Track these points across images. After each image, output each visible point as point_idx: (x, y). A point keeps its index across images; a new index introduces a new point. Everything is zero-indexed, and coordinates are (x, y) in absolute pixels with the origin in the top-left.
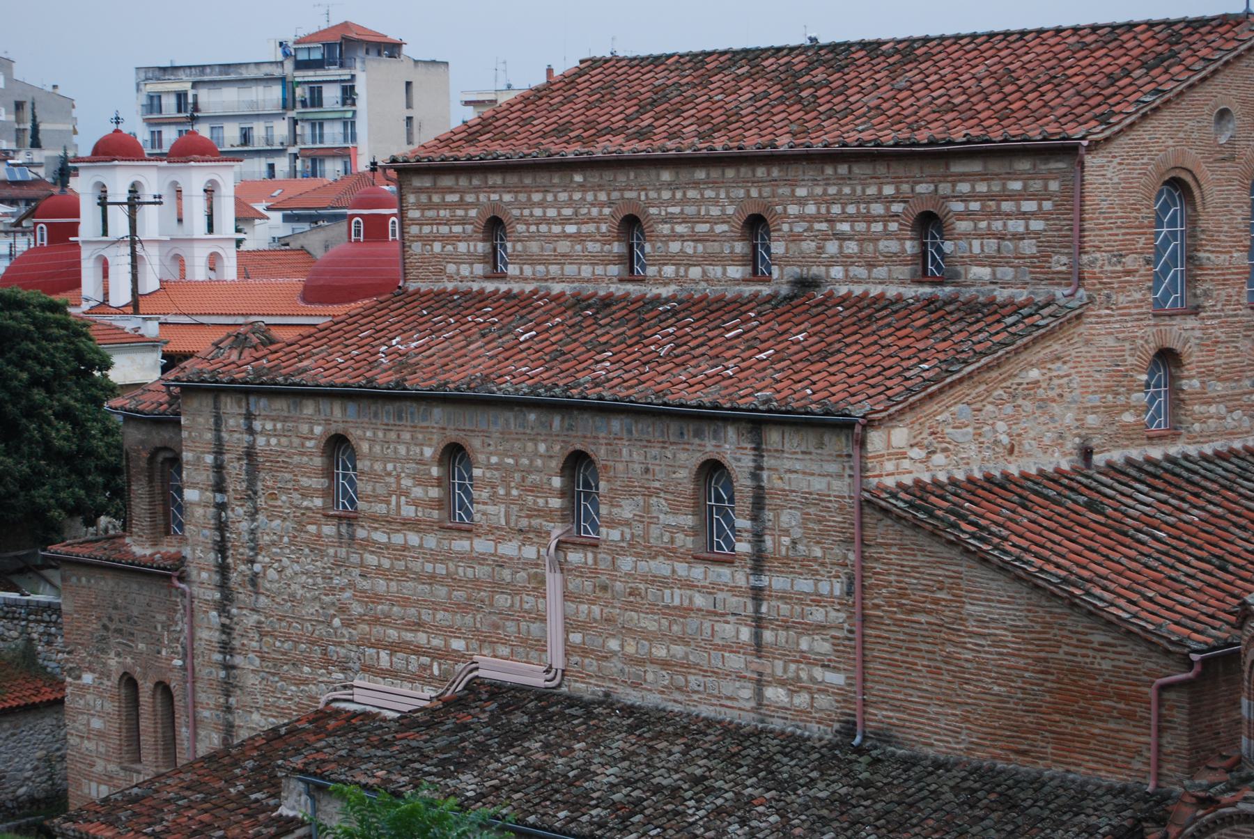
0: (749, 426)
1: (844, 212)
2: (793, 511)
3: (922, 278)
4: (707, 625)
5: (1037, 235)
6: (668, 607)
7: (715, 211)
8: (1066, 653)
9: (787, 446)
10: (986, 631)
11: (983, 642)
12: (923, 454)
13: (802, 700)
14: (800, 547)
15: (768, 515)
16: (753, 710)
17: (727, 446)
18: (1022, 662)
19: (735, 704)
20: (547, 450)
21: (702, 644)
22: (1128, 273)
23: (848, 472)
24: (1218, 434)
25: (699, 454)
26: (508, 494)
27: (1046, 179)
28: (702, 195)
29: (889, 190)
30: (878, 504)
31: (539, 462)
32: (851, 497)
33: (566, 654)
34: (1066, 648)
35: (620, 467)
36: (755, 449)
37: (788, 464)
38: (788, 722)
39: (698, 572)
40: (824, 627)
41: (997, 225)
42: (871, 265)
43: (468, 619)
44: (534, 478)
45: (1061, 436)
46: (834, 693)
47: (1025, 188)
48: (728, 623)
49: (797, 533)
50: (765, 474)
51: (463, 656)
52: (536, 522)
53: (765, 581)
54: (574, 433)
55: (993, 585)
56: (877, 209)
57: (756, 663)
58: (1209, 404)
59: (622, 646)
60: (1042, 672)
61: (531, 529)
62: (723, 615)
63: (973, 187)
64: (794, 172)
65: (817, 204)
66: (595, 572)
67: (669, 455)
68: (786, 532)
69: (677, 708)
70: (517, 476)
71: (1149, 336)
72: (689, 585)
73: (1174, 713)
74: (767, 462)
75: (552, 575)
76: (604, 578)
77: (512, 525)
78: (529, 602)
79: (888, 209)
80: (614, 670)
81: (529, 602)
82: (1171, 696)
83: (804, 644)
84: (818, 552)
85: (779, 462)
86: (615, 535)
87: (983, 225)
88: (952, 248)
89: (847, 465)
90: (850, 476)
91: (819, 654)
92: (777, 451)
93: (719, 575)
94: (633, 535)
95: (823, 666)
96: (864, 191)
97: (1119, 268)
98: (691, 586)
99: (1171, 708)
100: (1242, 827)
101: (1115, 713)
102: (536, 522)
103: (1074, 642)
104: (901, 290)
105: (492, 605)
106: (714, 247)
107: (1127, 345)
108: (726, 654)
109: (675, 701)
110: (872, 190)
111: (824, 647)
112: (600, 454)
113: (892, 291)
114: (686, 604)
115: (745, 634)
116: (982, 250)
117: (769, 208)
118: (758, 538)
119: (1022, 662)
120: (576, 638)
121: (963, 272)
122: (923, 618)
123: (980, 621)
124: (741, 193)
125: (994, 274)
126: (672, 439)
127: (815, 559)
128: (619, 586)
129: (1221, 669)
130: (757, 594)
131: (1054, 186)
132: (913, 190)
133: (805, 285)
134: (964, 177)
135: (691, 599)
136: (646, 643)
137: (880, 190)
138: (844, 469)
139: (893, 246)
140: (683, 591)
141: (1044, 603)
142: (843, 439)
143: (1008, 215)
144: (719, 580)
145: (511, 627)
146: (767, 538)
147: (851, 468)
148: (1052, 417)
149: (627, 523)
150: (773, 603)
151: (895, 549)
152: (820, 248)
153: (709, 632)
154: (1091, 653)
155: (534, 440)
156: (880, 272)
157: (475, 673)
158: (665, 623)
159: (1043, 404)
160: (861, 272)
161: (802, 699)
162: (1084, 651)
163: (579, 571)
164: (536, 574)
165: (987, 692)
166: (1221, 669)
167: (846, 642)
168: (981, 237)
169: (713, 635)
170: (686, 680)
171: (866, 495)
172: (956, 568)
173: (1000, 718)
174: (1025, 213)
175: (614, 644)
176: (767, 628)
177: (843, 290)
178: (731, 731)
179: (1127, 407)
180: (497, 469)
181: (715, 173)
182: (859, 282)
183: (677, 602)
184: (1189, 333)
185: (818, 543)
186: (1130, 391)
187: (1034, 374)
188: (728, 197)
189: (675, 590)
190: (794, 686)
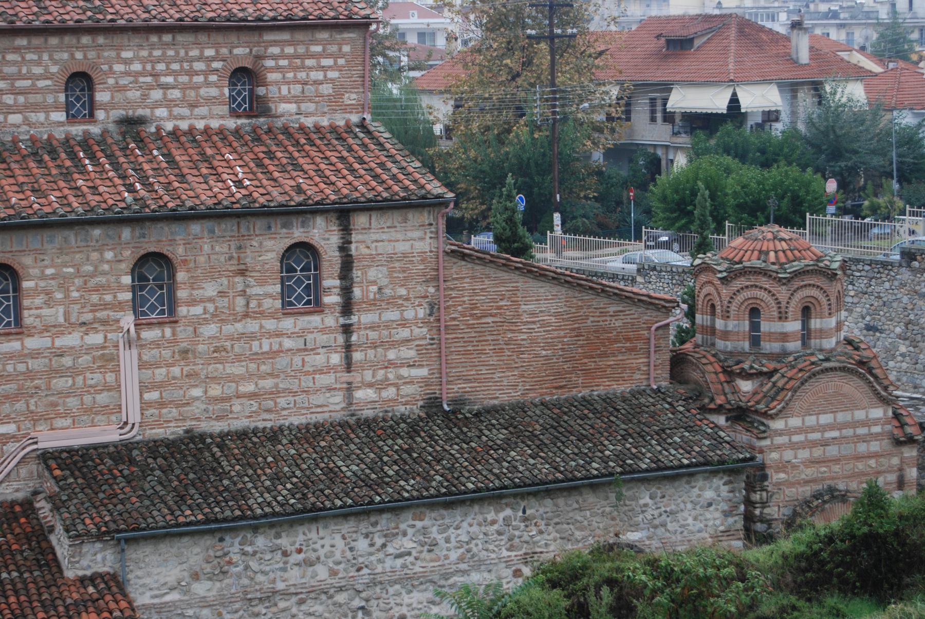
0: (336, 215)
1: (168, 68)
2: (380, 268)
3: (234, 114)
4: (297, 360)
5: (332, 80)
6: (256, 354)
7: (38, 70)
8: (592, 322)
9: (373, 226)
10: (537, 319)
11: (534, 326)
13: (390, 392)
14: (388, 291)
15: (357, 273)
16: (343, 409)
17: (316, 231)
18: (562, 333)
19: (325, 409)
20: (116, 257)
21: (293, 373)
23: (429, 235)
25: (287, 240)
26: (67, 296)
27: (340, 44)
28: (23, 58)
29: (209, 52)
30: (462, 253)
31: (106, 267)
32: (431, 252)
33: (142, 409)
34: (592, 319)
35: (202, 259)
36: (342, 230)
37: (374, 237)
38: (376, 411)
39: (288, 324)
40: (408, 341)
41: (302, 75)
42: (192, 106)
43: (20, 405)
44: (102, 280)
46: (418, 382)
47: (324, 50)
48: (319, 354)
49: (384, 282)
50: (353, 246)
51: (14, 437)
52: (101, 315)
53: (354, 319)
54: (146, 240)
55: (542, 290)
56: (199, 66)
57: (346, 377)
59: (206, 392)
60: (577, 336)
61: (95, 320)
62: (312, 350)
63: (282, 50)
64: (118, 40)
65: (143, 61)
66: (174, 341)
67: (255, 243)
68: (374, 283)
69: (269, 425)
70: (78, 282)
72: (279, 334)
73: (661, 341)
74: (355, 237)
75: (128, 352)
76: (184, 344)
77: (73, 320)
78: (95, 378)
79: (208, 66)
80: (196, 411)
81: (95, 378)
82: (660, 332)
83: (391, 355)
84: (403, 291)
85: (366, 236)
86: (198, 310)
87: (290, 75)
88: (265, 92)
89: (428, 231)
90: (431, 238)
91: (405, 359)
92: (365, 229)
93: (309, 322)
94: (216, 308)
95: (409, 366)
96: (187, 53)
98: (279, 334)
99: (659, 339)
101: (624, 350)
102: (101, 315)
103: (598, 314)
104: (222, 122)
105: (49, 389)
106: (39, 98)
108: (317, 376)
109: (264, 420)
110: (194, 53)
111: (409, 353)
112: (178, 252)
113: (215, 124)
114: (276, 347)
115: (336, 359)
116: (289, 92)
117: (95, 66)
118: (346, 291)
119: (562, 333)
120: (153, 396)
121: (273, 108)
122: (490, 320)
123: (533, 314)
124: (66, 56)
125: (299, 108)
126: (257, 232)
127: (400, 297)
128: (201, 348)
130: (347, 330)
131: (346, 49)
132: (231, 52)
133: (131, 125)
134: (275, 43)
135: (280, 345)
136: (234, 384)
137: (202, 52)
138: (425, 233)
139: (214, 92)
140: (271, 340)
141: (577, 295)
142: (426, 214)
143: (310, 68)
144: (308, 326)
145: (72, 402)
146: (355, 289)
147: (431, 232)
149: (211, 300)
150: (362, 333)
151: (468, 280)
152: (145, 96)
153: (300, 363)
154: (608, 318)
155: (101, 251)
156: (203, 110)
157: (35, 447)
158: (253, 366)
160: (185, 111)
161: (390, 392)
162: (604, 318)
163: (156, 344)
164: (103, 355)
165: (537, 356)
167: (429, 347)
168: (288, 83)
169: (303, 366)
170: (276, 403)
171: (453, 247)
172: (515, 285)
173: (546, 370)
174: (323, 67)
175: (197, 392)
176: (357, 351)
177: (169, 126)
178: (343, 425)
180: (53, 279)
181: (37, 41)
182: (183, 118)
183: (266, 348)
185: (402, 285)
188: (51, 58)
189: (264, 340)
190: (379, 386)
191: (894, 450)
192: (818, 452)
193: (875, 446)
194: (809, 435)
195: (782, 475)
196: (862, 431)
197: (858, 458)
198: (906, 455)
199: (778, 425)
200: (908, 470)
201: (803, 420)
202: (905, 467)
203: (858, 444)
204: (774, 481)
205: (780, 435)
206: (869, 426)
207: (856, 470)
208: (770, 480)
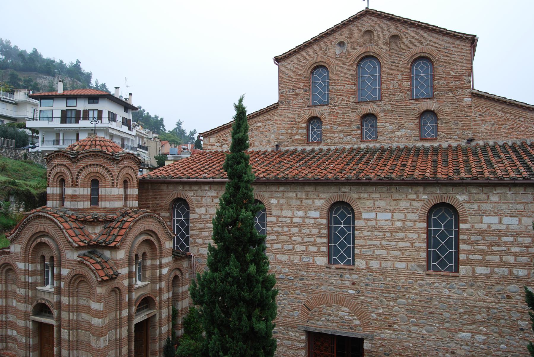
12: (220, 144)
22: (298, 94)
24: (338, 143)
45: (269, 141)
58: (335, 134)
71: (308, 113)
97: (293, 93)
107: (296, 116)
129: (150, 187)
148: (266, 136)
159: (262, 132)
166: (150, 187)
179: (297, 134)
184: (324, 111)
186: (298, 129)
187: (260, 124)
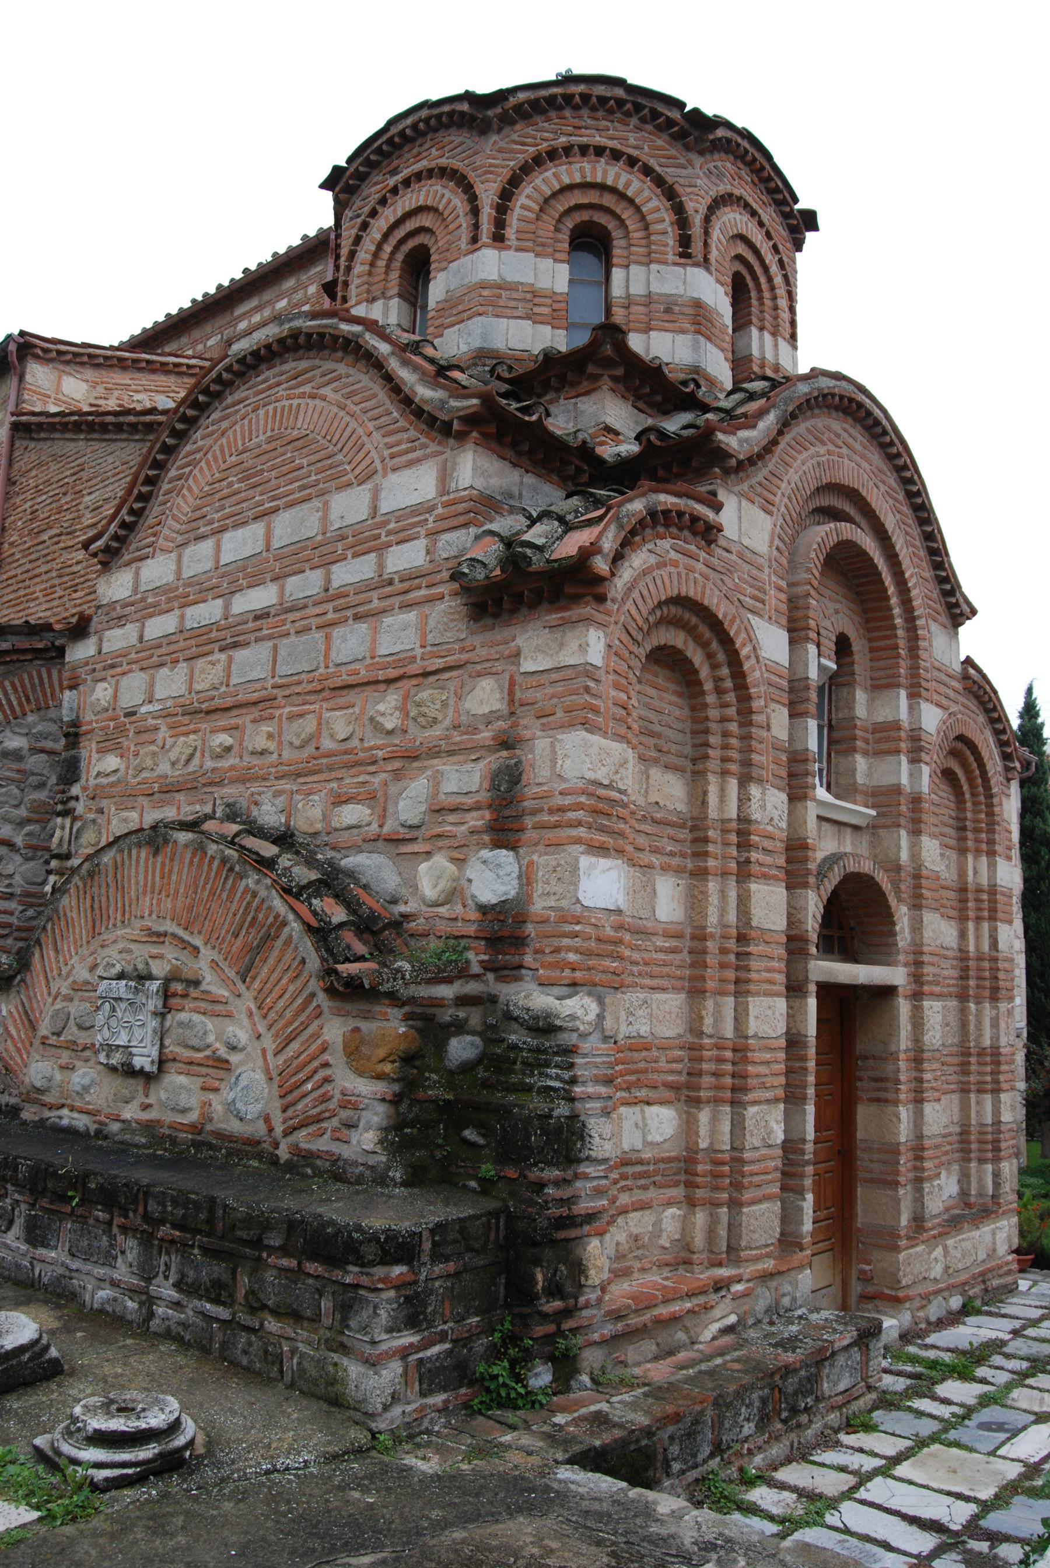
100: (237, 396)
191: (483, 644)
192: (209, 673)
193: (399, 634)
194: (189, 611)
195: (112, 762)
196: (352, 572)
197: (341, 689)
198: (528, 665)
199: (117, 587)
200: (542, 744)
201: (179, 562)
202: (529, 726)
203: (337, 632)
204: (92, 782)
205: (121, 621)
206: (381, 549)
207: (328, 744)
208: (83, 781)
